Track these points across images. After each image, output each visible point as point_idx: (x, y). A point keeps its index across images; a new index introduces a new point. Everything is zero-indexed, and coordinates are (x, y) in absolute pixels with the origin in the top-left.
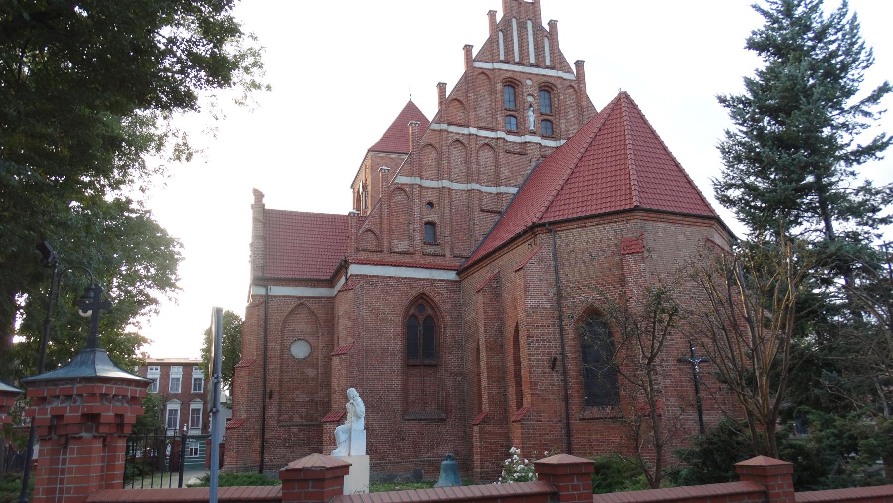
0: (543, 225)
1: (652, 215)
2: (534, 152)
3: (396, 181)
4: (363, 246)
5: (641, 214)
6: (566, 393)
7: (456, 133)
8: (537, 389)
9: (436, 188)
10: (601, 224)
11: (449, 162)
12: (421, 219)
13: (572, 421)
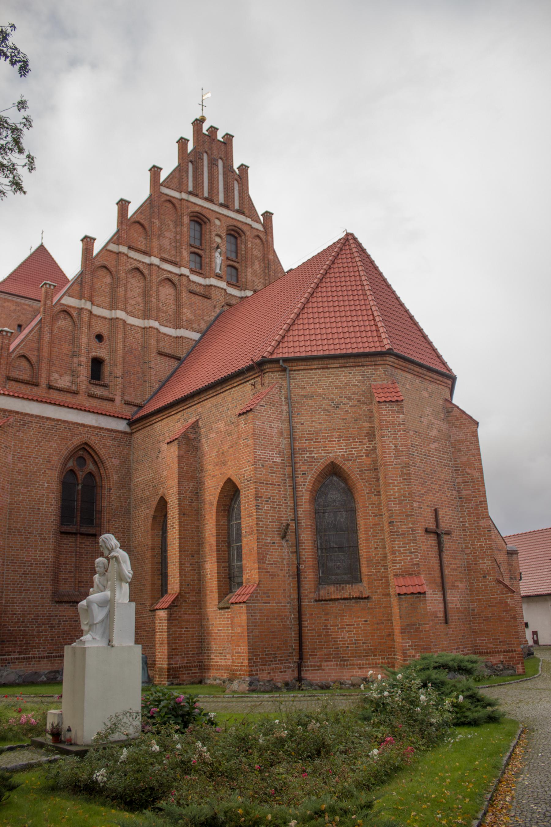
0: (277, 361)
1: (401, 363)
2: (218, 298)
3: (63, 301)
4: (15, 374)
5: (392, 360)
6: (298, 569)
7: (135, 260)
8: (265, 563)
9: (109, 319)
10: (346, 367)
11: (126, 291)
12: (88, 352)
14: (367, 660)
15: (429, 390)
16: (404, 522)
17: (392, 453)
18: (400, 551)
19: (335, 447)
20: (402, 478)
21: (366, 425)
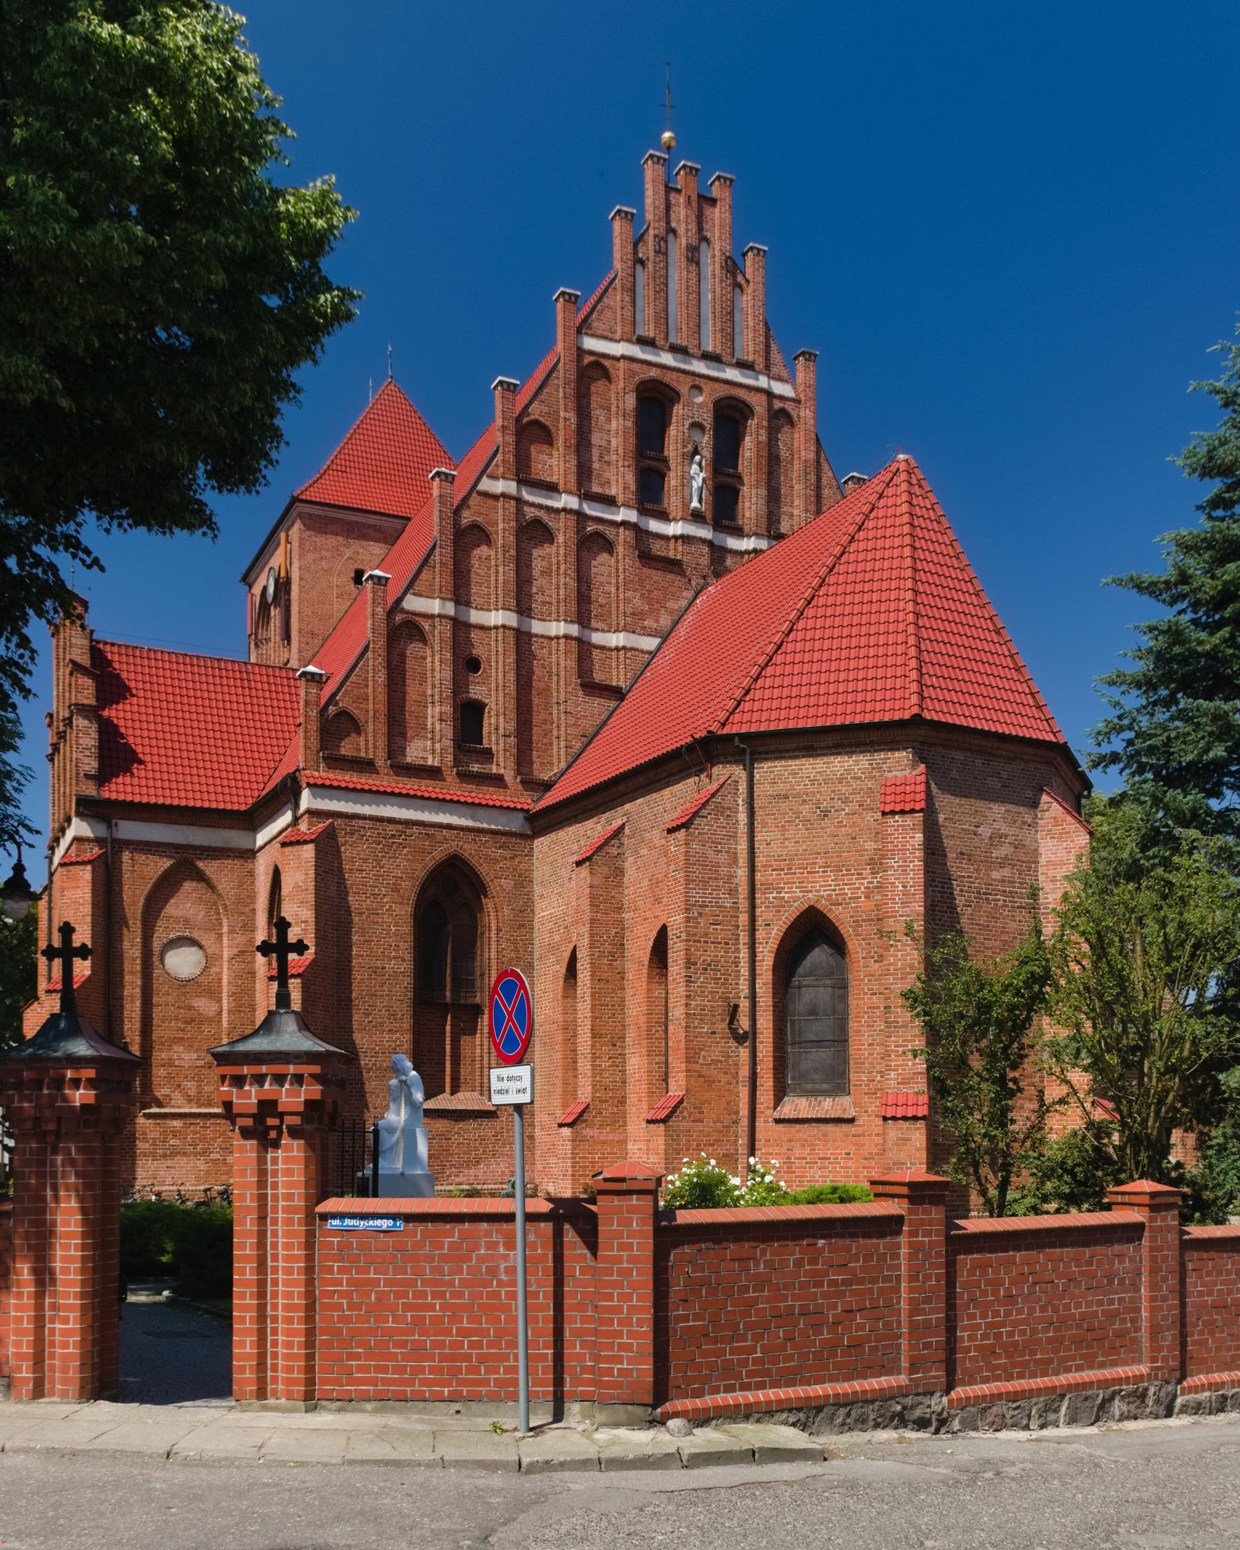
13: (759, 1123)
15: (1004, 775)
21: (870, 845)
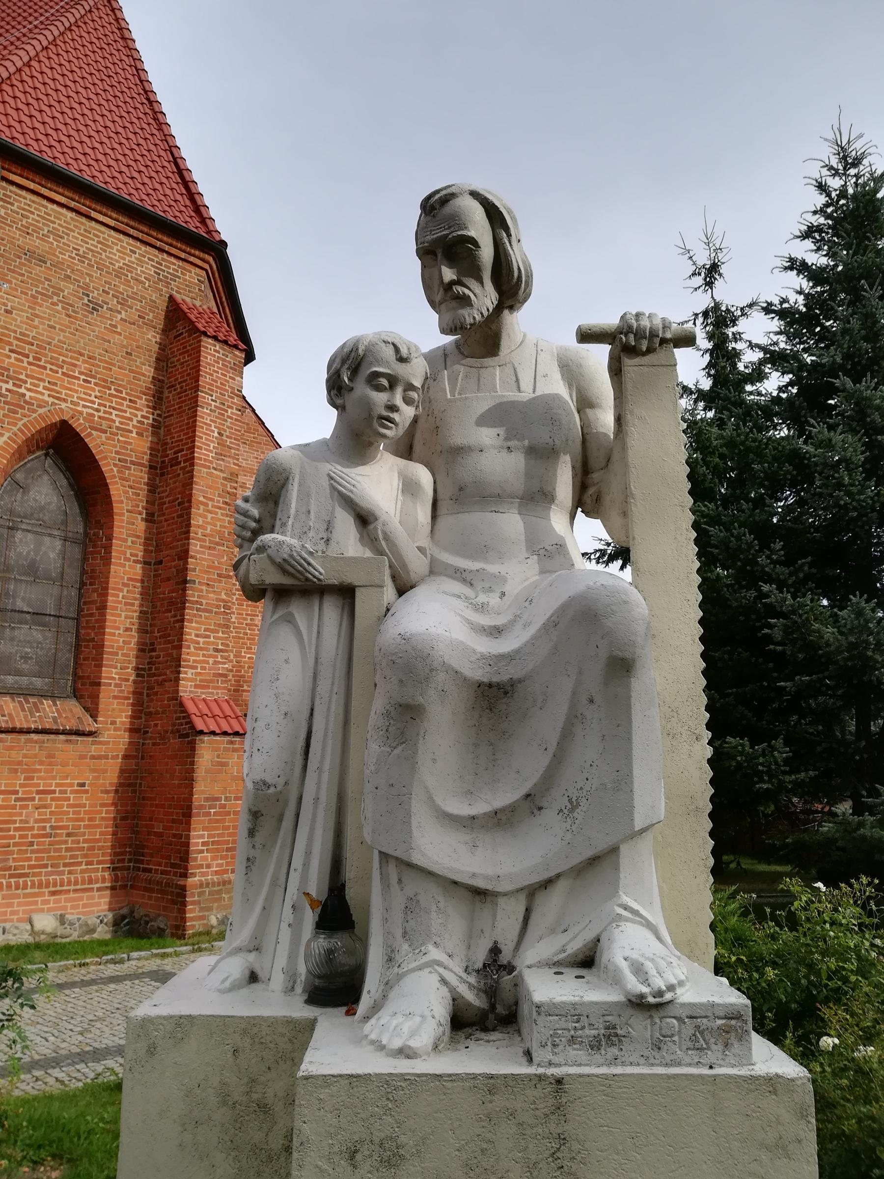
14: (70, 873)
16: (213, 587)
17: (212, 445)
18: (198, 643)
19: (76, 391)
20: (221, 500)
